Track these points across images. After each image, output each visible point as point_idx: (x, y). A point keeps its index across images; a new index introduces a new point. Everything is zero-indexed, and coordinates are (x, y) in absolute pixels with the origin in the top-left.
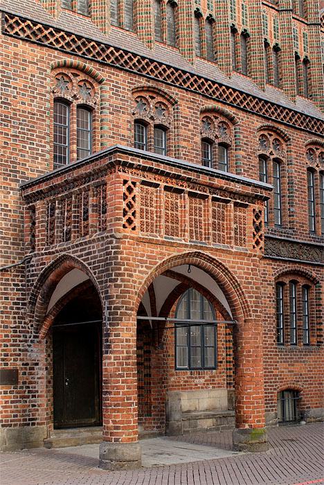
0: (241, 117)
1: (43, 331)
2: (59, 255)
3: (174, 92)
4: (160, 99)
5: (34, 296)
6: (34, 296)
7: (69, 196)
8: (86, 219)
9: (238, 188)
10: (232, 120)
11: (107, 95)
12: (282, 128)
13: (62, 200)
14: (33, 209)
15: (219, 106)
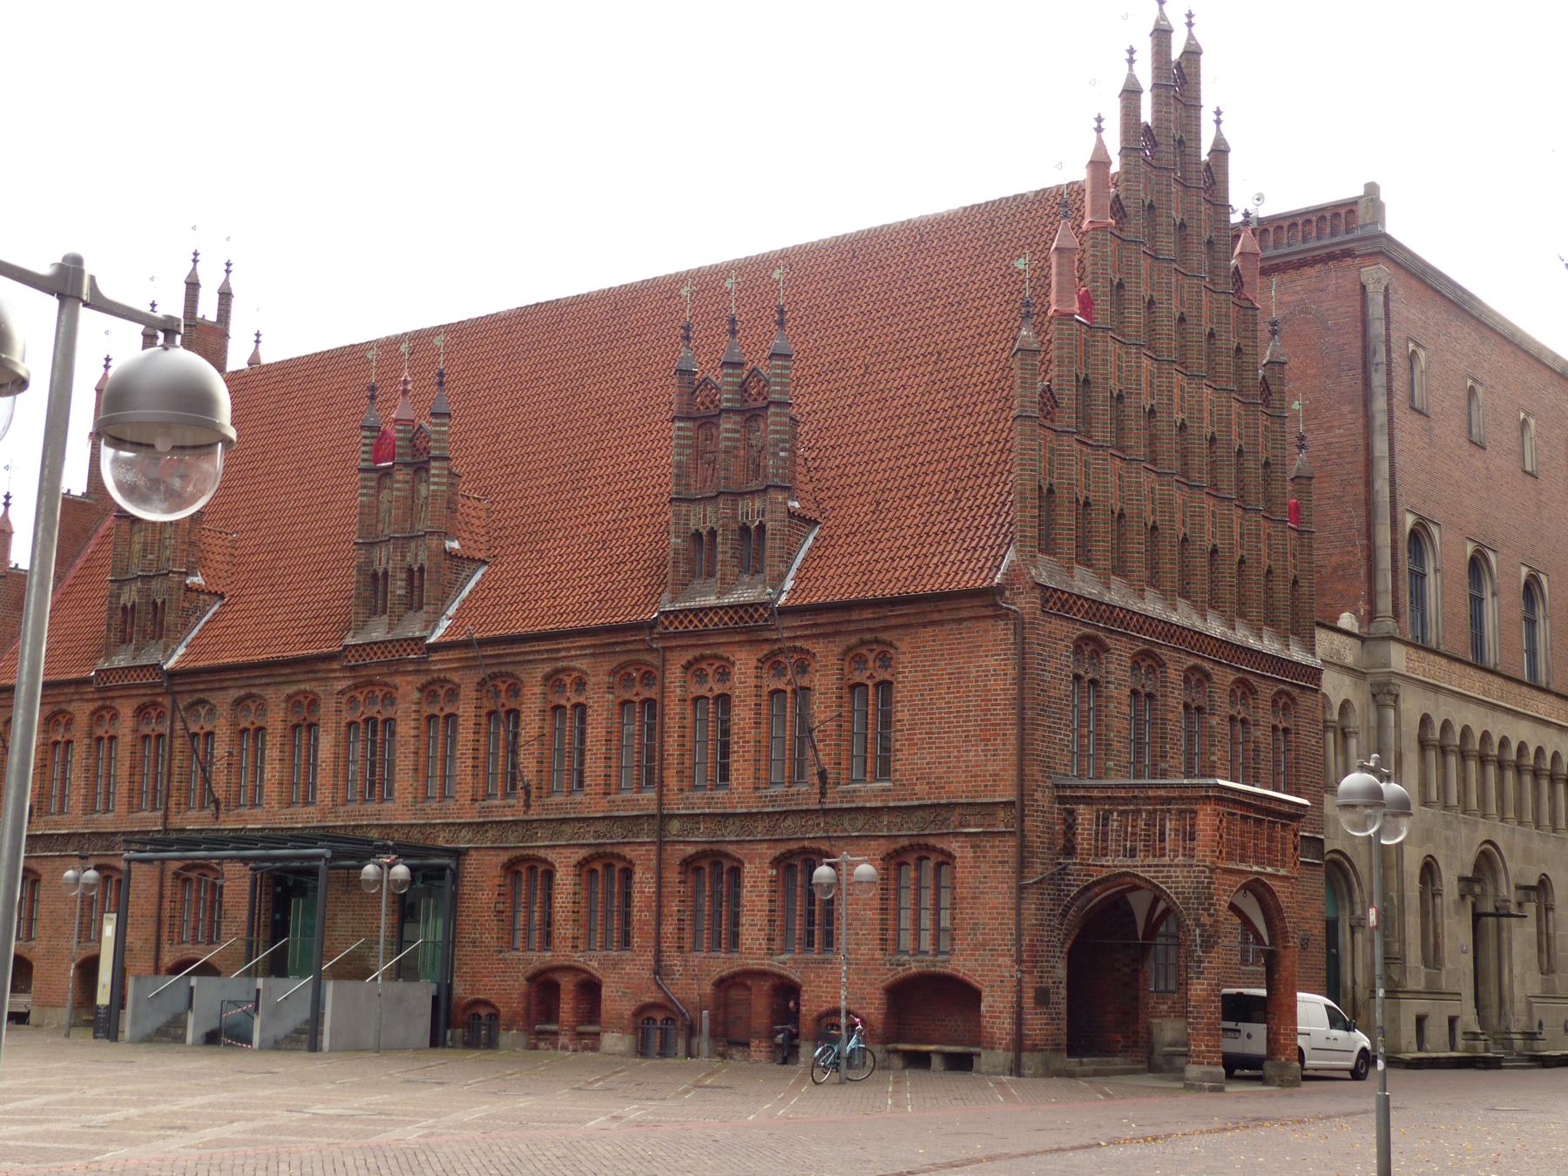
0: (1217, 673)
1: (1068, 945)
2: (1117, 871)
3: (1165, 654)
4: (1149, 662)
5: (1068, 907)
6: (1068, 907)
7: (1139, 811)
8: (1162, 840)
9: (1286, 809)
10: (1208, 676)
11: (1112, 667)
12: (1251, 678)
13: (1121, 813)
14: (1071, 812)
15: (1199, 662)
